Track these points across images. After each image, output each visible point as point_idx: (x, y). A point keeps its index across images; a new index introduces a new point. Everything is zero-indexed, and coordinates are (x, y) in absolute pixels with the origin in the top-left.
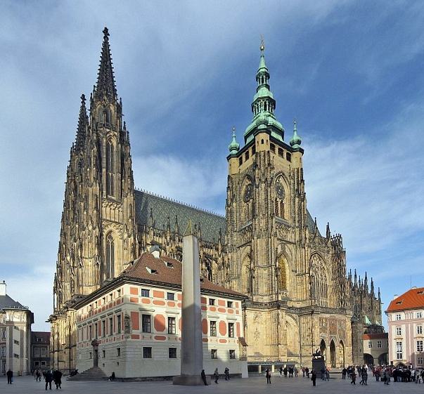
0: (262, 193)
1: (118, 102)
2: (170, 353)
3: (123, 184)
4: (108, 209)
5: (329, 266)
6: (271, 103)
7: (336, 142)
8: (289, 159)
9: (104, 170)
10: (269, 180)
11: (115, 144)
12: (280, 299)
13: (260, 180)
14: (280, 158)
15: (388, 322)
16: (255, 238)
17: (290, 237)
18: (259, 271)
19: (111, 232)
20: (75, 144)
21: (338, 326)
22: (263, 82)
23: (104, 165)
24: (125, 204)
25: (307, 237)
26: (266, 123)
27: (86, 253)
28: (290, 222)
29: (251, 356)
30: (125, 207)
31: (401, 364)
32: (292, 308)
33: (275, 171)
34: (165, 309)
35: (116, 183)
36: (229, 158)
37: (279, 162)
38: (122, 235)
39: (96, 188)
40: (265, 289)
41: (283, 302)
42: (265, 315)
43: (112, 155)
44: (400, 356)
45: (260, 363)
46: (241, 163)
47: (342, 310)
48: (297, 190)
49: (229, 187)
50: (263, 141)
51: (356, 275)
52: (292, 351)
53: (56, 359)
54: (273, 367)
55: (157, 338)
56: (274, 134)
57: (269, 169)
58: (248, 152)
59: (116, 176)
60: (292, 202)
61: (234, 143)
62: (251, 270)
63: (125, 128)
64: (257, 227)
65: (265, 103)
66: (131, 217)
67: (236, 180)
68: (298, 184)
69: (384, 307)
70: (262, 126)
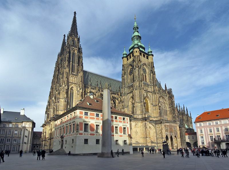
0: (137, 71)
1: (78, 37)
2: (96, 142)
3: (79, 68)
4: (72, 78)
5: (167, 102)
6: (139, 37)
7: (166, 52)
8: (147, 58)
9: (71, 63)
10: (140, 66)
11: (76, 53)
12: (146, 116)
14: (144, 58)
15: (196, 127)
16: (135, 90)
17: (149, 89)
18: (136, 104)
19: (72, 87)
20: (60, 53)
21: (173, 129)
22: (136, 30)
23: (71, 60)
24: (79, 76)
25: (157, 89)
26: (137, 45)
27: (61, 96)
28: (149, 83)
29: (134, 143)
30: (79, 77)
31: (204, 147)
32: (152, 120)
33: (142, 63)
34: (95, 121)
35: (76, 68)
36: (123, 58)
37: (143, 59)
38: (77, 89)
39: (67, 70)
40: (140, 112)
41: (148, 118)
42: (140, 124)
43: (75, 57)
44: (203, 143)
45: (138, 147)
46: (128, 60)
47: (175, 122)
48: (152, 70)
49: (123, 69)
50: (136, 51)
51: (179, 106)
52: (153, 140)
53: (43, 145)
54: (144, 148)
55: (91, 134)
56: (141, 49)
57: (139, 62)
58: (131, 56)
59: (76, 65)
61: (125, 52)
62: (133, 104)
63: (80, 47)
64: (135, 85)
65: (137, 37)
66: (81, 81)
67: (126, 66)
68: (152, 68)
69: (193, 120)
70: (136, 46)
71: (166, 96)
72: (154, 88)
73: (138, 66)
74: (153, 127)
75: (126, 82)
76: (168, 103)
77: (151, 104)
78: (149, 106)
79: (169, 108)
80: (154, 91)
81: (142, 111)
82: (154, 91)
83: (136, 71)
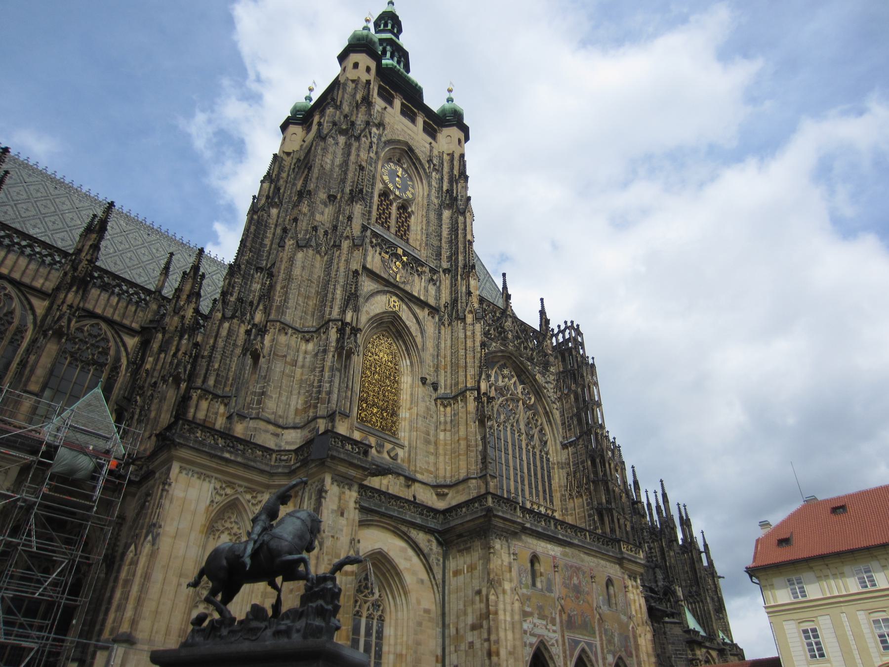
13: (335, 124)
28: (423, 254)
40: (297, 402)
48: (449, 191)
60: (433, 216)
68: (451, 182)
71: (546, 366)
72: (454, 285)
73: (353, 124)
74: (415, 560)
75: (267, 242)
76: (557, 414)
77: (424, 381)
78: (405, 397)
79: (565, 446)
80: (455, 301)
81: (315, 396)
82: (455, 301)
83: (331, 150)
